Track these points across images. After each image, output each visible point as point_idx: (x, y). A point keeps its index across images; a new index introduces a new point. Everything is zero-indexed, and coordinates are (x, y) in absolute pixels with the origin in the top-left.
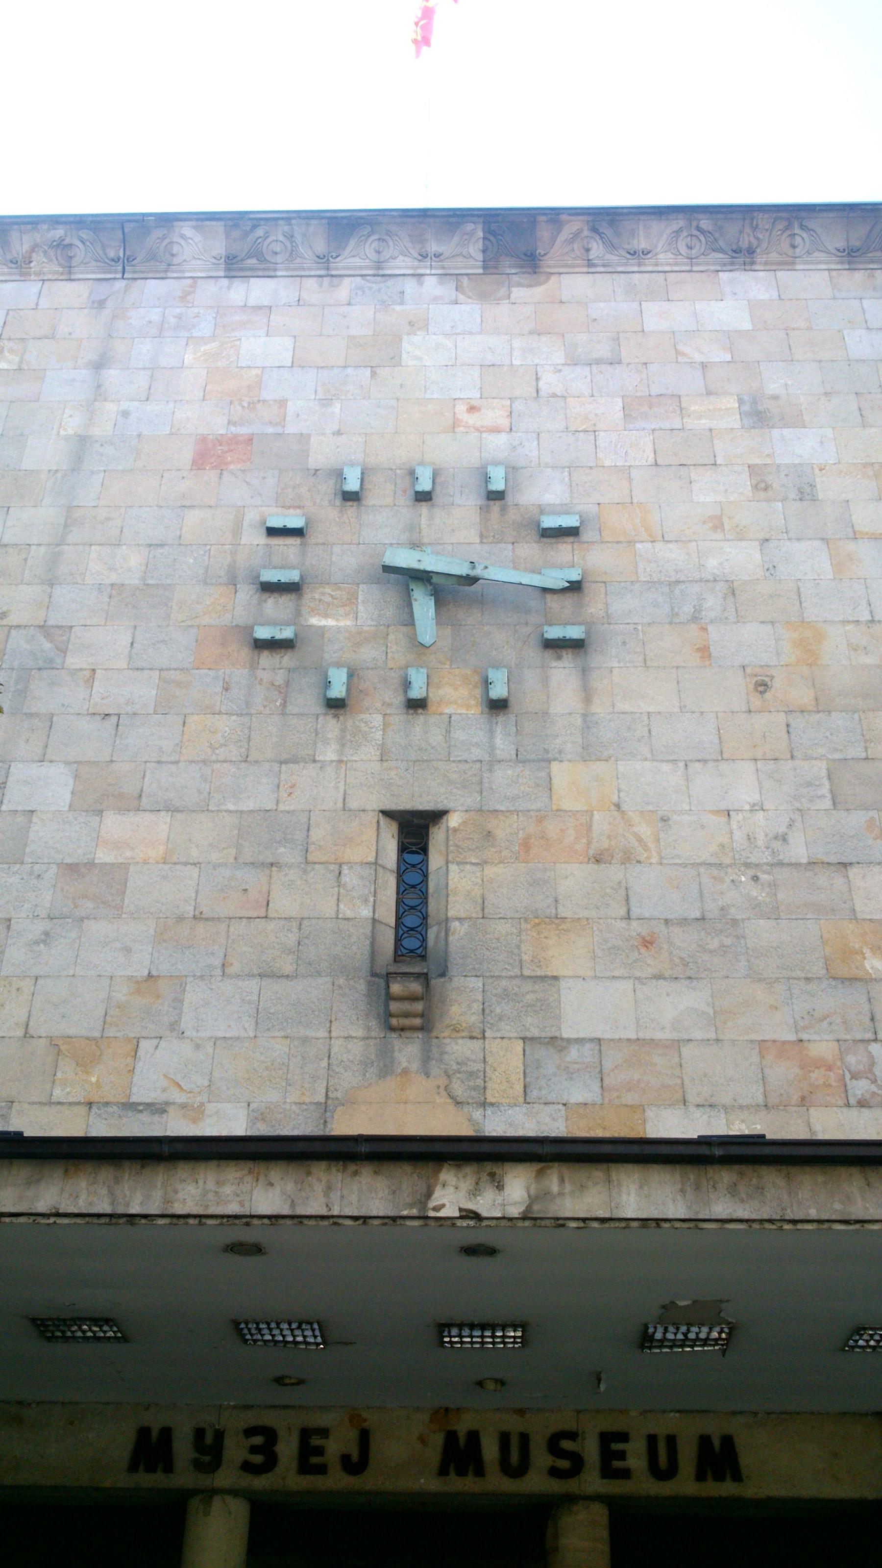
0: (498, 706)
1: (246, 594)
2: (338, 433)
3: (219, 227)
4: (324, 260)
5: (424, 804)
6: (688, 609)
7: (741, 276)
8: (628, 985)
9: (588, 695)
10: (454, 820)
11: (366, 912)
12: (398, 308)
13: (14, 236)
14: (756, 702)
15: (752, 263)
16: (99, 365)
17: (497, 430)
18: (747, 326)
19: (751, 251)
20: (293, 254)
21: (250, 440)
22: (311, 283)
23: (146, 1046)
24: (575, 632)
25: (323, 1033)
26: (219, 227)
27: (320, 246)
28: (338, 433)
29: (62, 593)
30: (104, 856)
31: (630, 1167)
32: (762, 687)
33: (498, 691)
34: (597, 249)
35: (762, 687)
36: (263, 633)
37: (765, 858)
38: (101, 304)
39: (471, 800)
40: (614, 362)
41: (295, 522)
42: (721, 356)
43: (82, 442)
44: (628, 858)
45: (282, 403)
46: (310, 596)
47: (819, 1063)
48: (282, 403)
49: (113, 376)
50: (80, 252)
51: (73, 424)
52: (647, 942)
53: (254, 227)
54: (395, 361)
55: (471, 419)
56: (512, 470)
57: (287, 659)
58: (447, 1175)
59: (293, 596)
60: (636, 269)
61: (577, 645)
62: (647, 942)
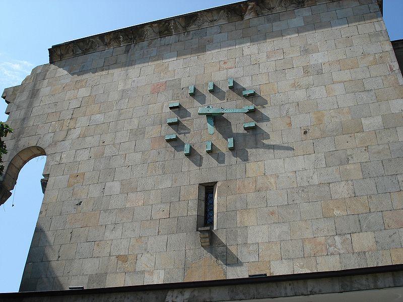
1: (165, 127)
2: (189, 76)
4: (185, 28)
6: (285, 112)
7: (301, 10)
8: (267, 226)
10: (218, 185)
12: (205, 38)
13: (105, 37)
14: (304, 136)
15: (304, 5)
19: (303, 2)
23: (139, 256)
25: (184, 249)
26: (156, 25)
27: (183, 24)
28: (189, 76)
29: (119, 134)
31: (216, 287)
32: (305, 133)
35: (305, 133)
37: (306, 184)
39: (224, 178)
43: (123, 91)
44: (267, 189)
47: (320, 243)
51: (120, 87)
52: (272, 213)
53: (165, 23)
55: (225, 66)
58: (170, 293)
59: (176, 125)
60: (271, 13)
62: (272, 213)
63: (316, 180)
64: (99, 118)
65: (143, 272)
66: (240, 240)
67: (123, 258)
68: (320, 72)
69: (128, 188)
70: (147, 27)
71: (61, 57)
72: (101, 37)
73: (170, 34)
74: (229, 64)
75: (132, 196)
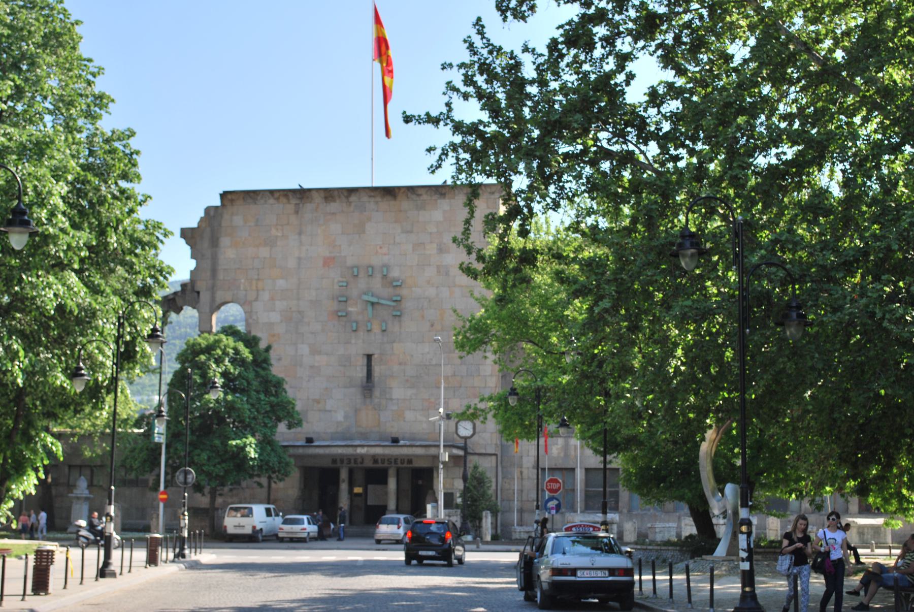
0: (384, 331)
3: (322, 194)
5: (370, 353)
9: (400, 328)
10: (376, 356)
11: (361, 375)
16: (300, 234)
17: (385, 254)
18: (441, 219)
20: (339, 197)
21: (334, 258)
22: (344, 204)
24: (398, 313)
27: (346, 194)
30: (316, 364)
32: (432, 326)
33: (384, 328)
34: (409, 194)
35: (432, 326)
36: (340, 314)
38: (297, 212)
40: (411, 232)
41: (344, 284)
42: (435, 230)
45: (340, 246)
46: (349, 302)
48: (340, 246)
49: (303, 237)
50: (291, 197)
52: (407, 381)
54: (364, 232)
55: (379, 251)
56: (387, 266)
57: (345, 319)
61: (399, 316)
63: (434, 362)
64: (281, 283)
65: (330, 411)
66: (388, 396)
67: (318, 402)
68: (447, 274)
69: (315, 351)
70: (314, 192)
71: (232, 201)
72: (272, 192)
73: (334, 201)
74: (385, 250)
75: (317, 358)
